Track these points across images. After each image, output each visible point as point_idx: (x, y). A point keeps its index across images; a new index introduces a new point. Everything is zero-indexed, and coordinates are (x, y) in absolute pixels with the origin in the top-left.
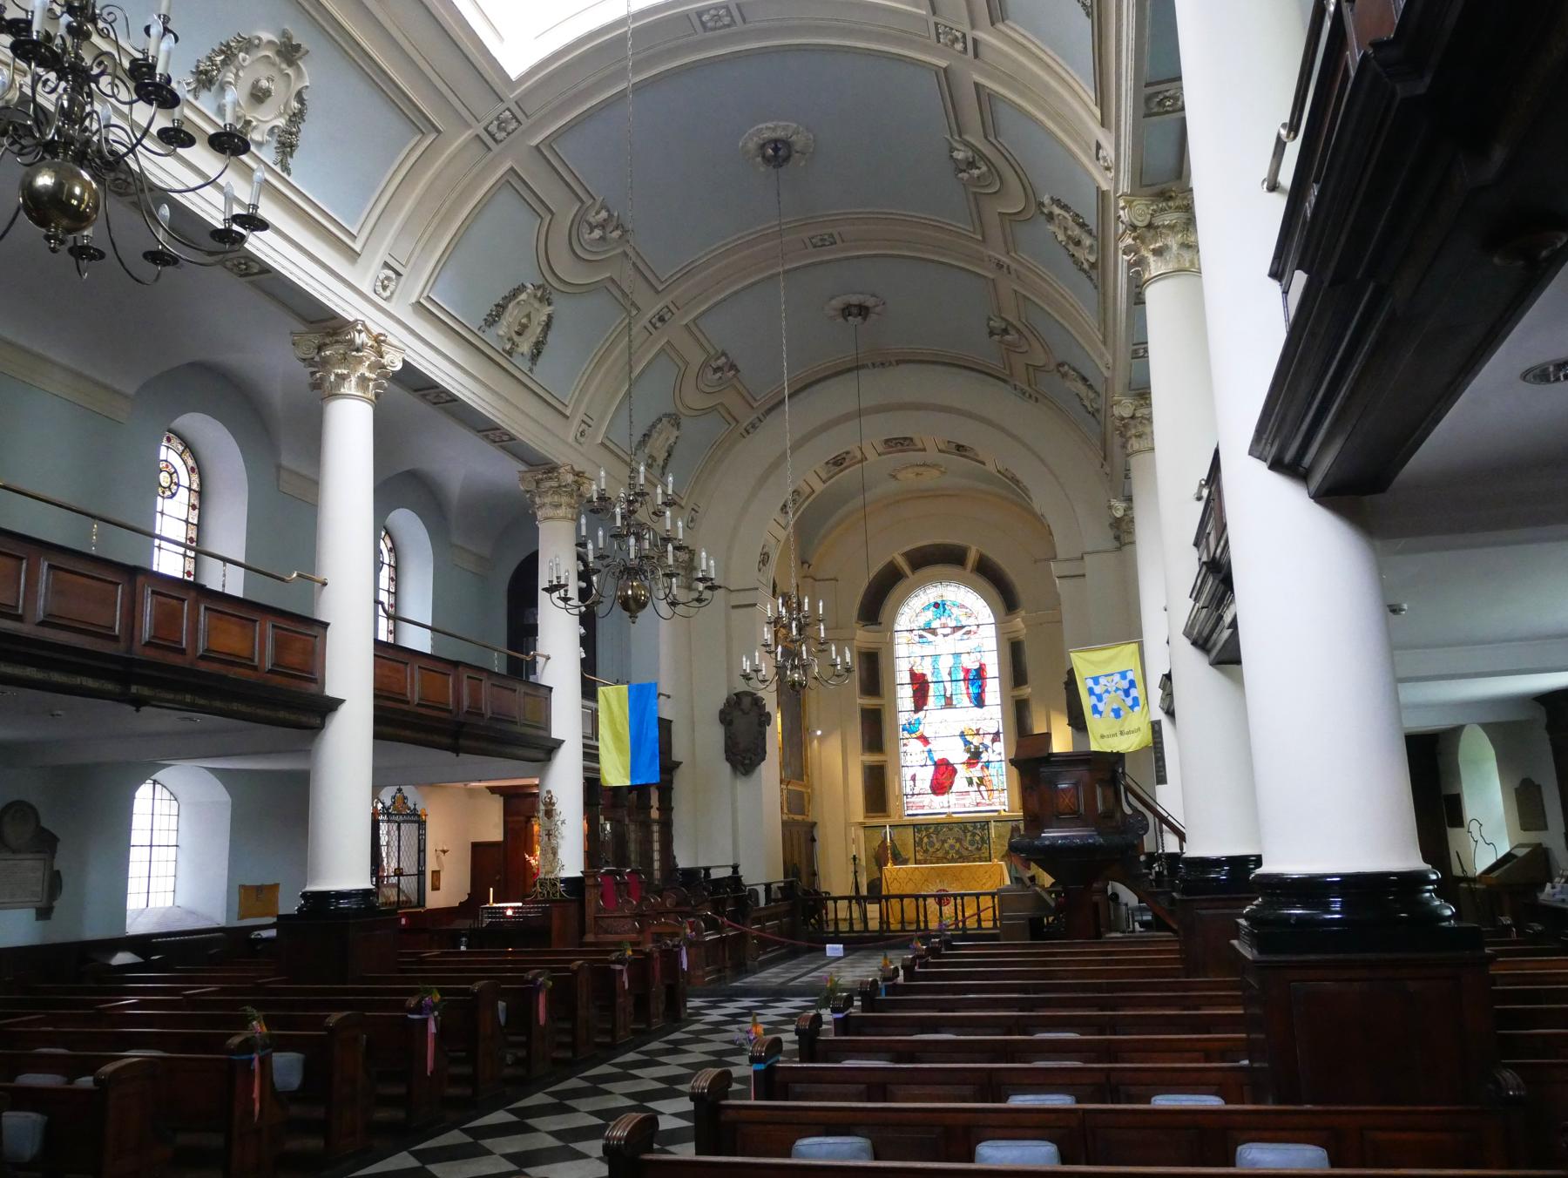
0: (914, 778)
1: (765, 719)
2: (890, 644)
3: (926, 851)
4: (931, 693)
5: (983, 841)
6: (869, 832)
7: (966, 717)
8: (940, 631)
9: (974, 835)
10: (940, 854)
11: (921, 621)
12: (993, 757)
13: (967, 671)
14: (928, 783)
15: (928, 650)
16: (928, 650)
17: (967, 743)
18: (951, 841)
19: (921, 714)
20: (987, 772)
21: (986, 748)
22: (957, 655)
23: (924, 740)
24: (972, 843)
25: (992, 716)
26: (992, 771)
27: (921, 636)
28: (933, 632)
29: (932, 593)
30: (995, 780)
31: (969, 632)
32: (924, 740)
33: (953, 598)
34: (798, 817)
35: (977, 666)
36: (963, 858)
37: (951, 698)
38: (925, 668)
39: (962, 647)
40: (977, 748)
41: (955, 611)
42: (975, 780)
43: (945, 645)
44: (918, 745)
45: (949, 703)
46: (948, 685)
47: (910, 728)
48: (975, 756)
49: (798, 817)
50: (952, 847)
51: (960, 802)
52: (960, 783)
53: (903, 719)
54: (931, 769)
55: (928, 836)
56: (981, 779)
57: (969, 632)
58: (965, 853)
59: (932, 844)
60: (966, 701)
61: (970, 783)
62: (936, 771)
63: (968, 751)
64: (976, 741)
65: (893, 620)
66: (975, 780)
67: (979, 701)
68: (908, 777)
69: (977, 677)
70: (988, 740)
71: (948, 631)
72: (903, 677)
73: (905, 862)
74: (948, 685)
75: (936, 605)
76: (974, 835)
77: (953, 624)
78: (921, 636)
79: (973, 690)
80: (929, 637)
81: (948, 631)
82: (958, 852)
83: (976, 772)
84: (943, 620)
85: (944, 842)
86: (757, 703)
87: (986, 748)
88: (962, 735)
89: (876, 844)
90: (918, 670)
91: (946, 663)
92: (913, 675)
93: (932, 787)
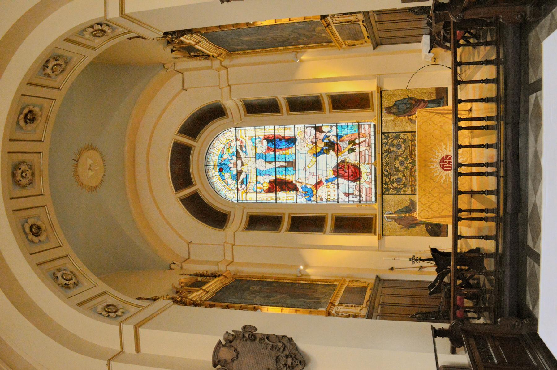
0: (347, 194)
1: (249, 334)
2: (246, 205)
3: (405, 185)
4: (283, 177)
5: (395, 138)
6: (386, 232)
7: (302, 152)
8: (239, 169)
9: (392, 145)
10: (408, 174)
11: (231, 182)
12: (334, 133)
13: (269, 149)
14: (353, 184)
15: (252, 177)
16: (252, 177)
17: (322, 152)
18: (397, 164)
19: (299, 185)
20: (345, 138)
21: (326, 137)
22: (257, 156)
23: (318, 184)
24: (399, 146)
25: (301, 130)
26: (344, 133)
27: (242, 183)
28: (240, 173)
29: (214, 173)
30: (351, 131)
31: (241, 147)
32: (318, 184)
33: (217, 157)
34: (368, 293)
35: (265, 142)
36: (411, 155)
37: (288, 162)
38: (265, 181)
39: (251, 152)
40: (326, 144)
41: (225, 156)
42: (350, 146)
43: (249, 166)
44: (322, 192)
45: (292, 164)
46: (278, 164)
47: (309, 193)
48: (332, 146)
49: (368, 293)
50: (402, 163)
51: (367, 159)
52: (353, 158)
53: (301, 199)
54: (341, 180)
55: (392, 182)
56: (350, 142)
57: (241, 147)
58: (407, 152)
59: (399, 180)
60: (291, 151)
61: (353, 150)
62: (343, 177)
63: (328, 151)
64: (321, 145)
65: (230, 203)
66: (350, 146)
67: (292, 141)
68: (346, 199)
69: (272, 140)
70: (321, 136)
71: (239, 162)
72: (272, 195)
73: (413, 203)
74: (278, 164)
75: (221, 170)
76: (392, 145)
77: (235, 158)
78: (242, 183)
79: (283, 144)
80: (243, 176)
81: (239, 162)
82: (406, 159)
83: (345, 146)
84: (232, 165)
85: (398, 170)
86: (231, 340)
87: (326, 137)
88: (316, 155)
89: (396, 226)
90: (266, 186)
91: (262, 165)
92: (269, 190)
93: (355, 181)
